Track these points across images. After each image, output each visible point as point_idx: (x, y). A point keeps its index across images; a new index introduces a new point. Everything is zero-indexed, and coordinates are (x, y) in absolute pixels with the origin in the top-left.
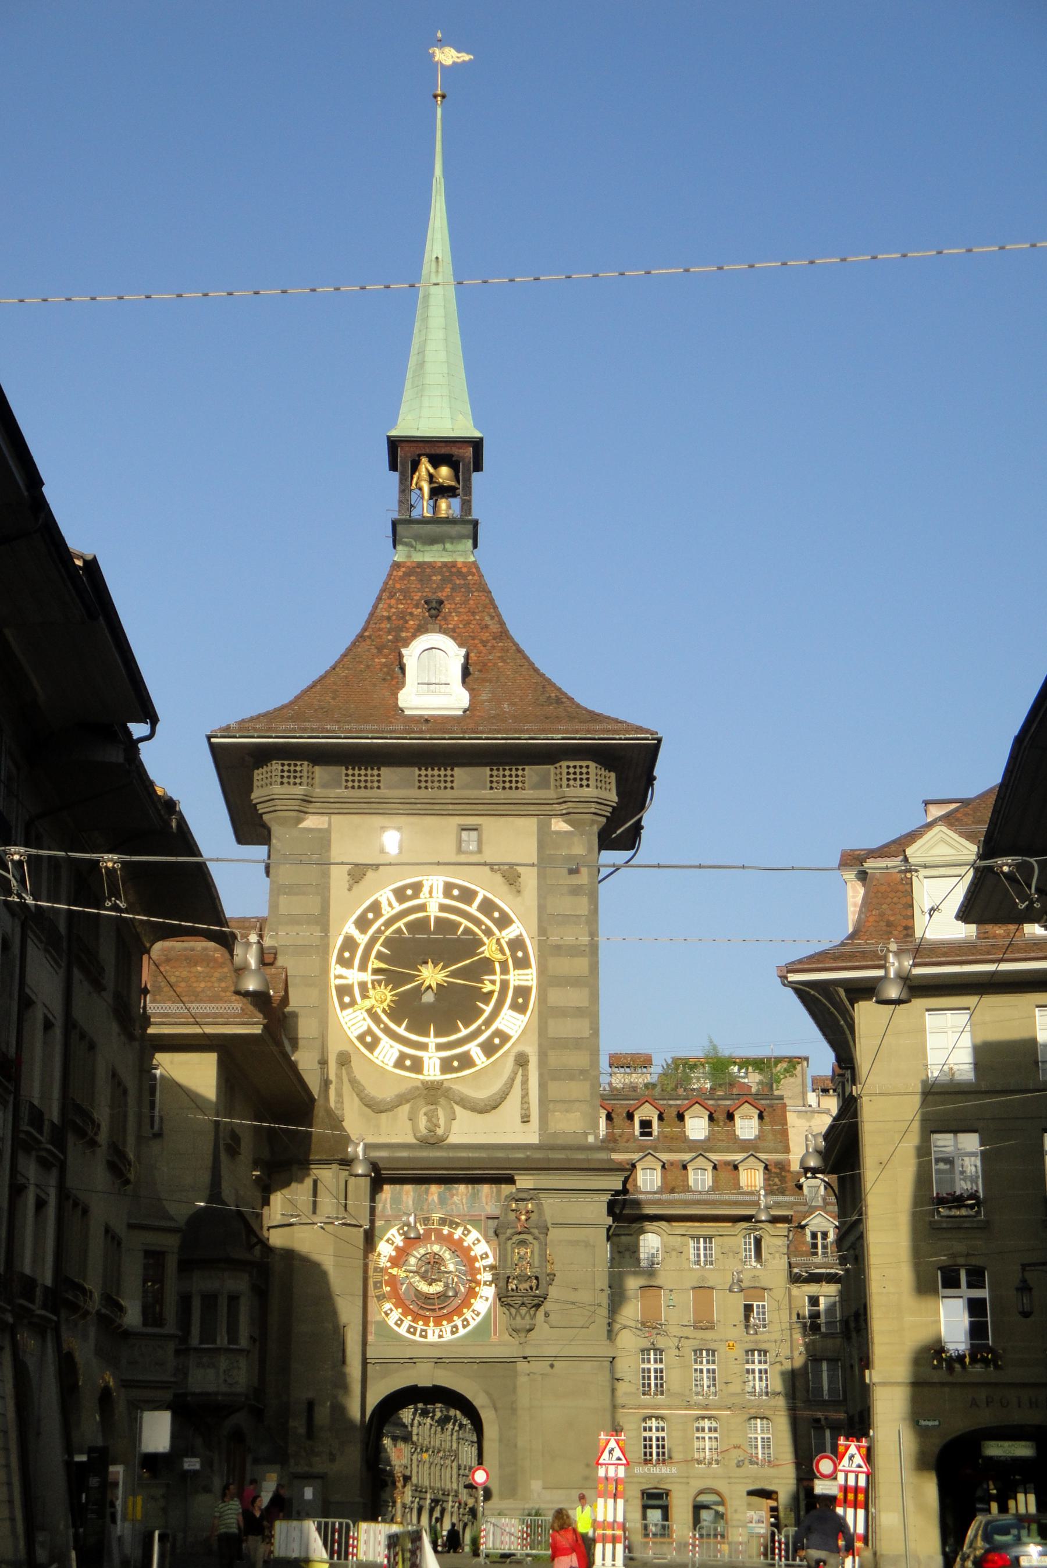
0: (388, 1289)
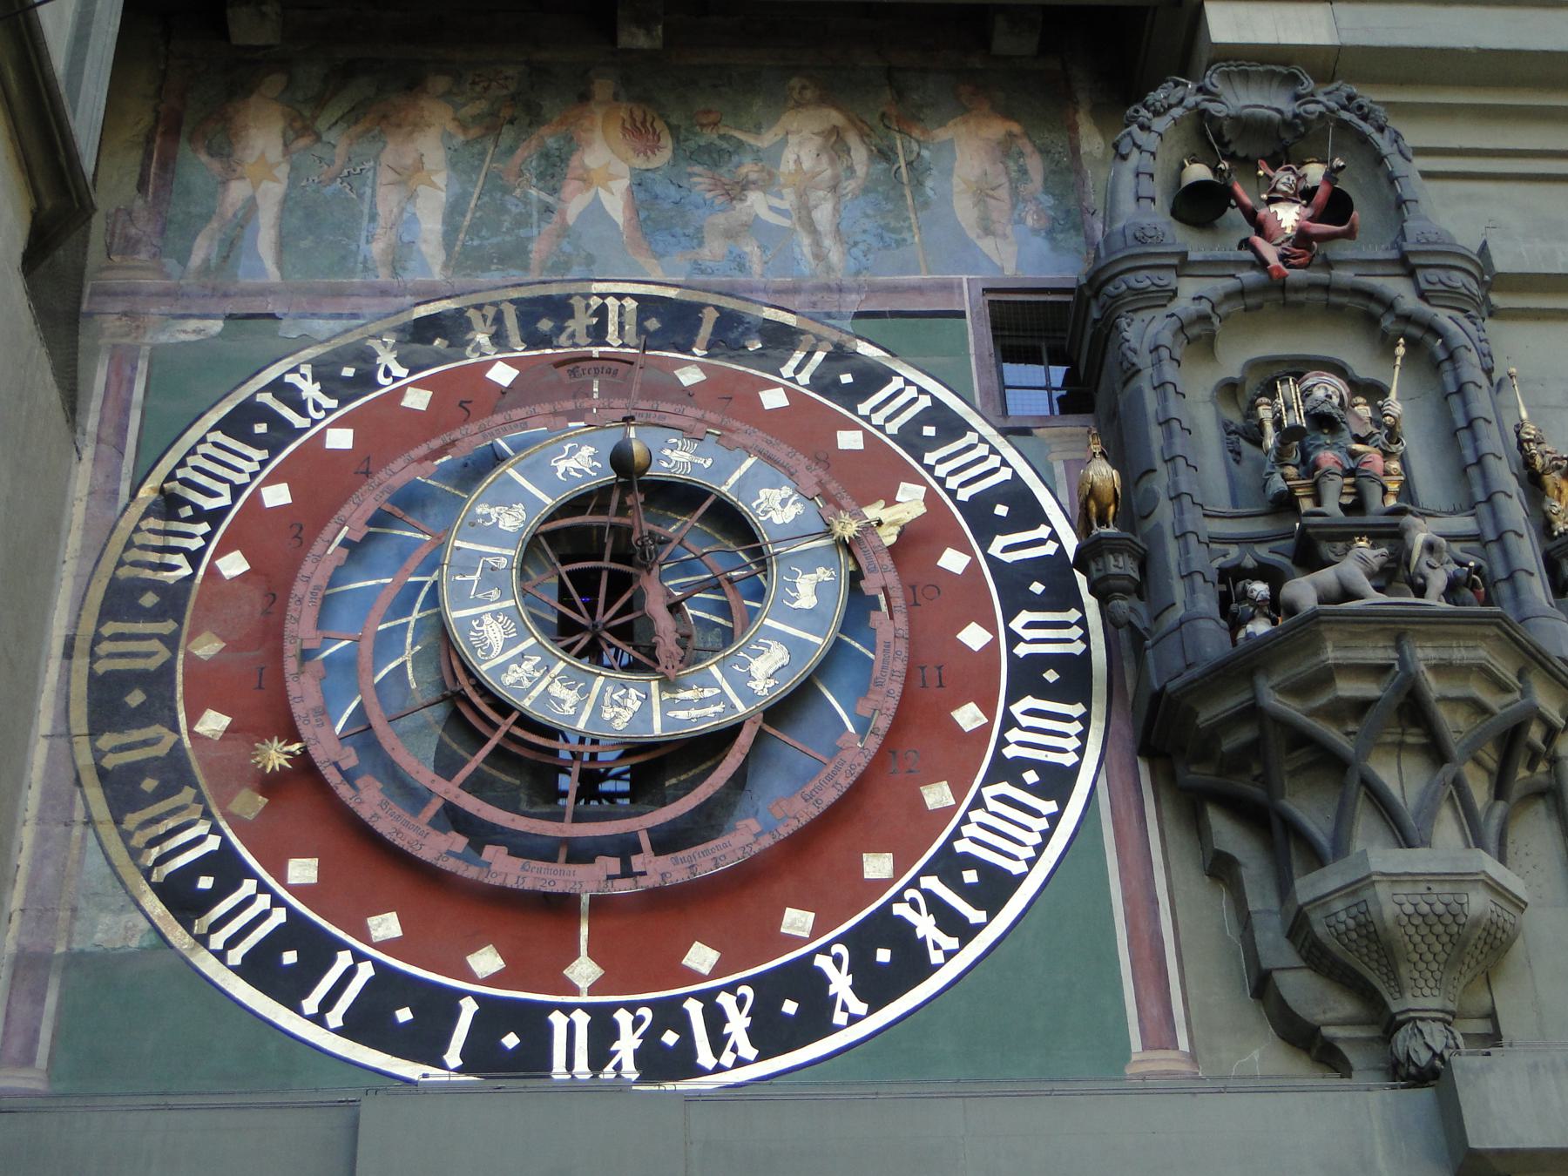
0: (214, 723)
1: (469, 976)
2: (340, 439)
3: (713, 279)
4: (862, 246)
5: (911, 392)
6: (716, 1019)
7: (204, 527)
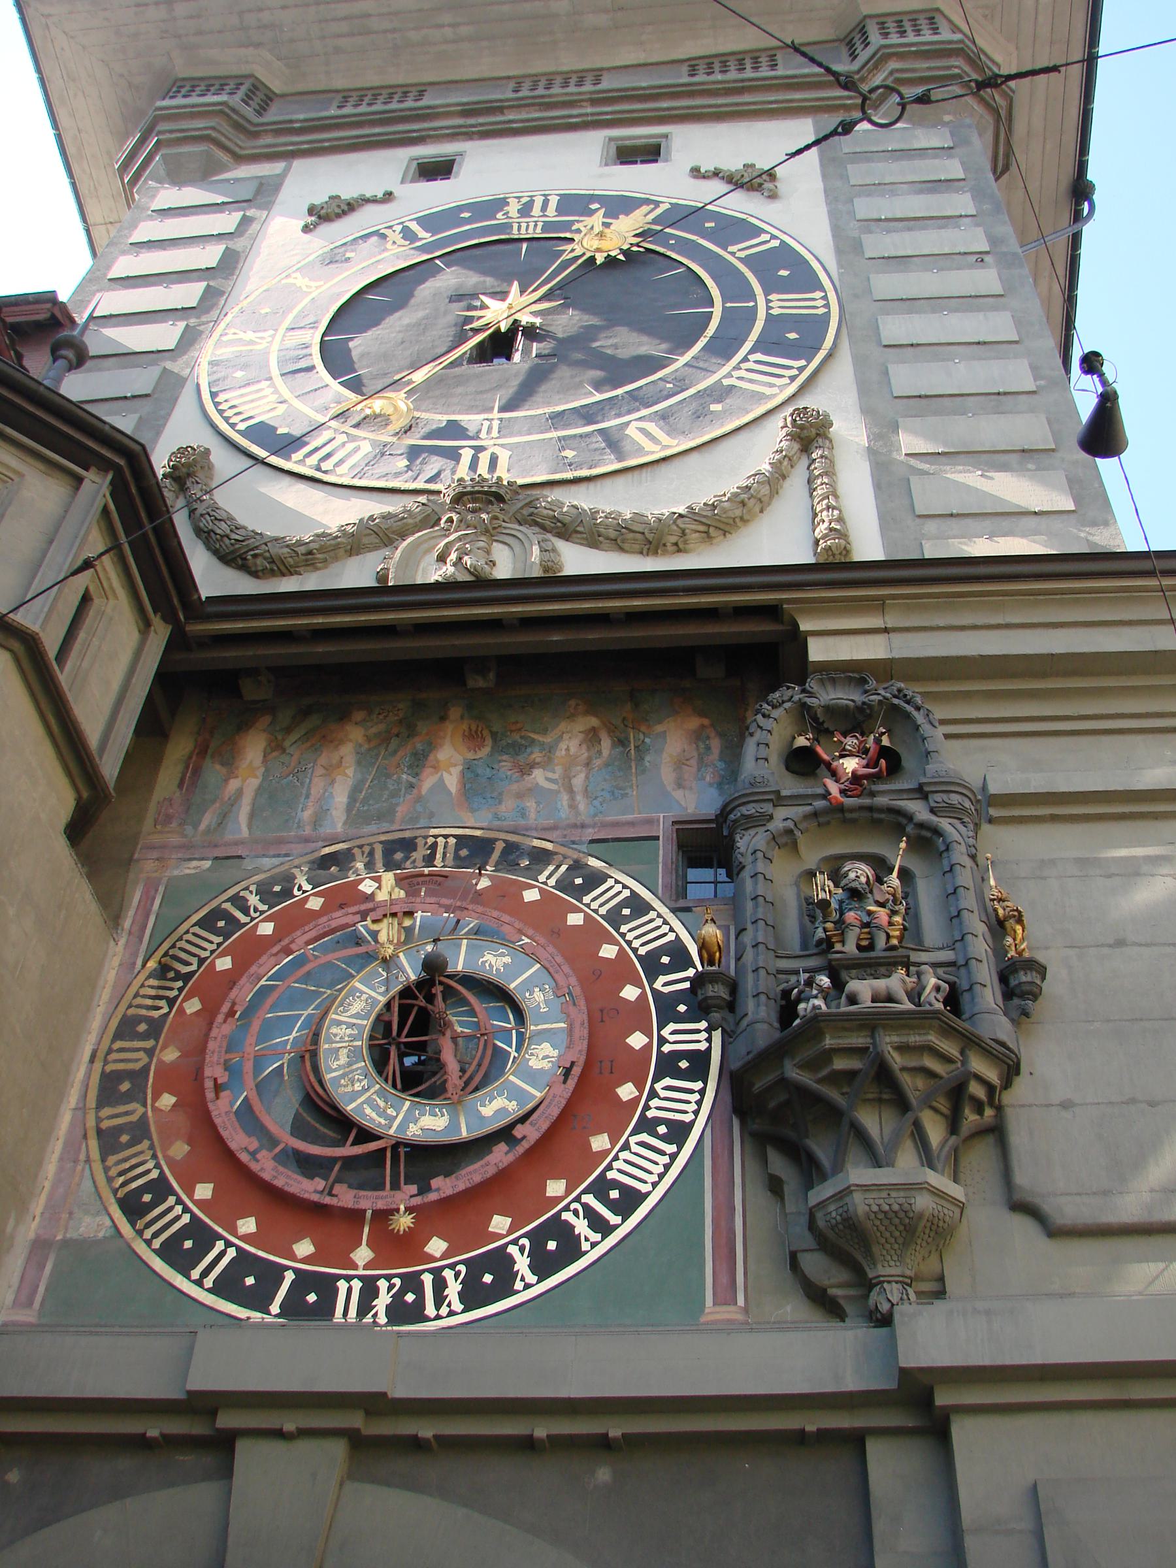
0: (167, 1100)
1: (292, 1256)
2: (267, 929)
3: (505, 823)
4: (600, 799)
5: (619, 887)
6: (440, 1285)
7: (180, 984)
